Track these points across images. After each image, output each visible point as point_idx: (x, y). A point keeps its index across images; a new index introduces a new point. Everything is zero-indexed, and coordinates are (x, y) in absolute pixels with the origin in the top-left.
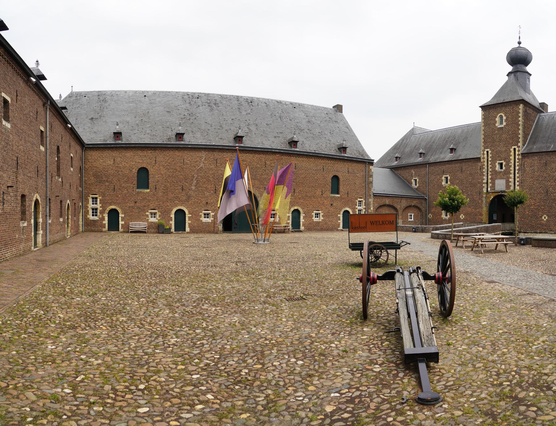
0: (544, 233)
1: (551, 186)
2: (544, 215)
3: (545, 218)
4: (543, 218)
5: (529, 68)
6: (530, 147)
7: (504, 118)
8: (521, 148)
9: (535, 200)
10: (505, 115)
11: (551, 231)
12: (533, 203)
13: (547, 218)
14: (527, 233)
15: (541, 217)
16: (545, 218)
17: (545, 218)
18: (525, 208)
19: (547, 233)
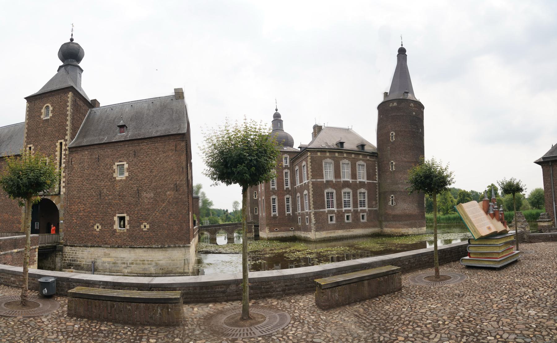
0: (97, 247)
1: (105, 187)
2: (97, 224)
3: (98, 227)
4: (95, 227)
5: (81, 65)
6: (80, 140)
7: (51, 108)
8: (68, 142)
9: (85, 205)
10: (52, 106)
11: (106, 244)
12: (82, 209)
13: (100, 227)
14: (75, 246)
15: (93, 226)
16: (98, 227)
17: (98, 227)
18: (72, 215)
19: (100, 247)
